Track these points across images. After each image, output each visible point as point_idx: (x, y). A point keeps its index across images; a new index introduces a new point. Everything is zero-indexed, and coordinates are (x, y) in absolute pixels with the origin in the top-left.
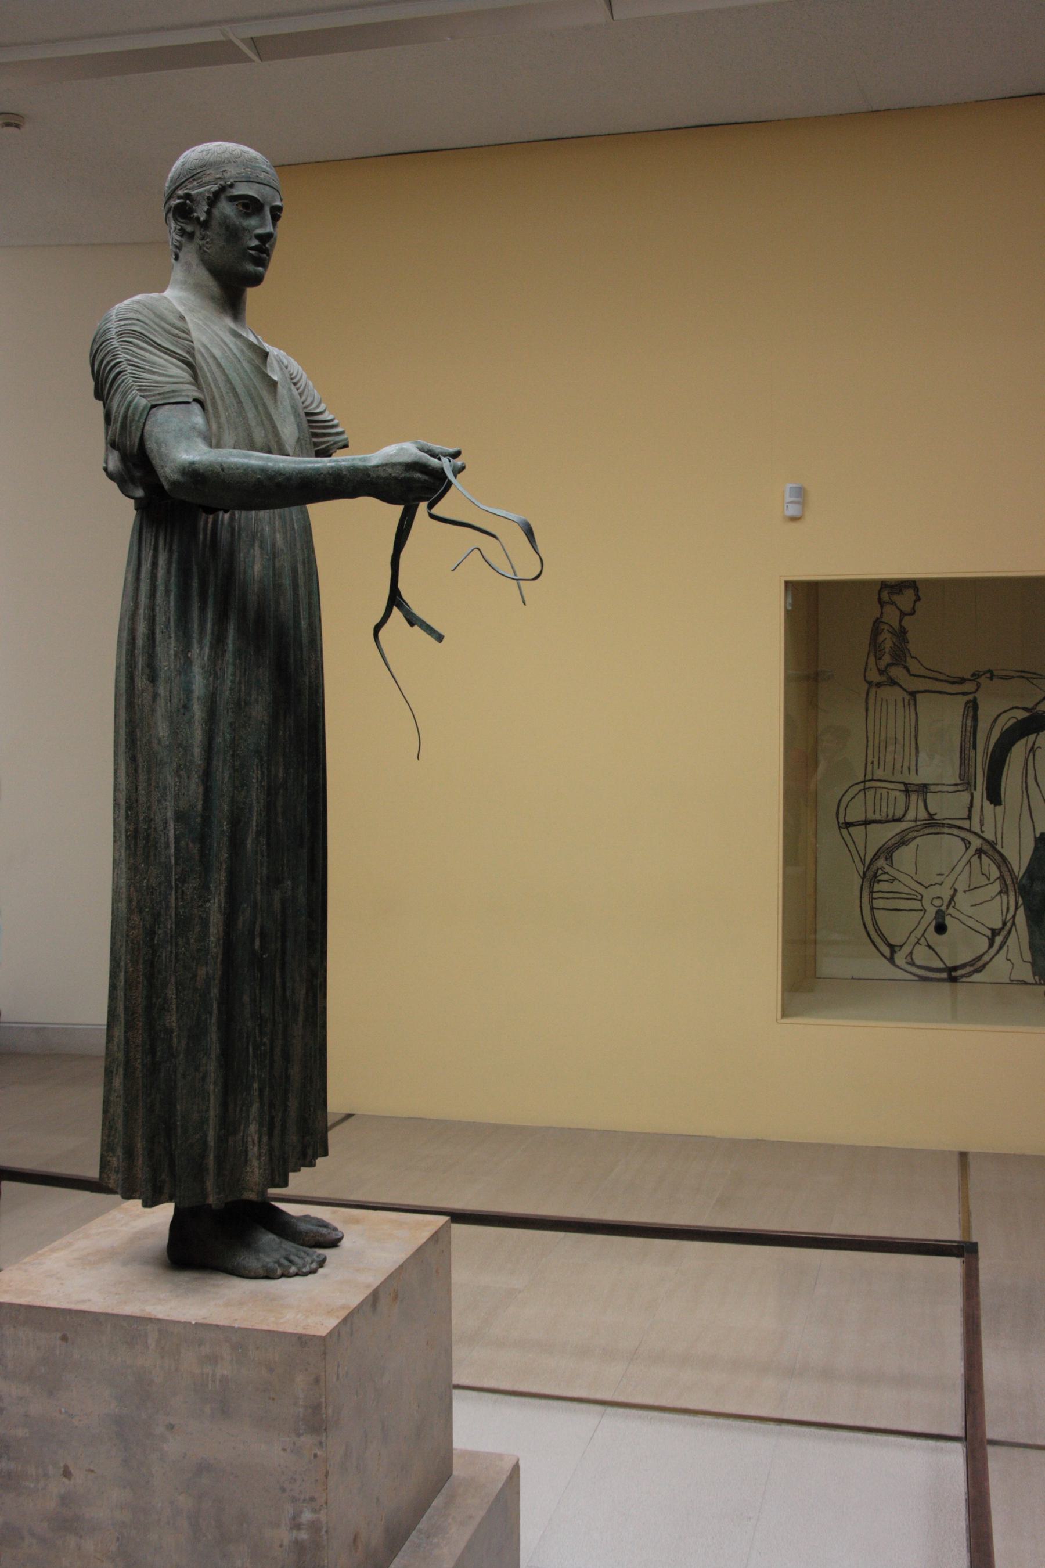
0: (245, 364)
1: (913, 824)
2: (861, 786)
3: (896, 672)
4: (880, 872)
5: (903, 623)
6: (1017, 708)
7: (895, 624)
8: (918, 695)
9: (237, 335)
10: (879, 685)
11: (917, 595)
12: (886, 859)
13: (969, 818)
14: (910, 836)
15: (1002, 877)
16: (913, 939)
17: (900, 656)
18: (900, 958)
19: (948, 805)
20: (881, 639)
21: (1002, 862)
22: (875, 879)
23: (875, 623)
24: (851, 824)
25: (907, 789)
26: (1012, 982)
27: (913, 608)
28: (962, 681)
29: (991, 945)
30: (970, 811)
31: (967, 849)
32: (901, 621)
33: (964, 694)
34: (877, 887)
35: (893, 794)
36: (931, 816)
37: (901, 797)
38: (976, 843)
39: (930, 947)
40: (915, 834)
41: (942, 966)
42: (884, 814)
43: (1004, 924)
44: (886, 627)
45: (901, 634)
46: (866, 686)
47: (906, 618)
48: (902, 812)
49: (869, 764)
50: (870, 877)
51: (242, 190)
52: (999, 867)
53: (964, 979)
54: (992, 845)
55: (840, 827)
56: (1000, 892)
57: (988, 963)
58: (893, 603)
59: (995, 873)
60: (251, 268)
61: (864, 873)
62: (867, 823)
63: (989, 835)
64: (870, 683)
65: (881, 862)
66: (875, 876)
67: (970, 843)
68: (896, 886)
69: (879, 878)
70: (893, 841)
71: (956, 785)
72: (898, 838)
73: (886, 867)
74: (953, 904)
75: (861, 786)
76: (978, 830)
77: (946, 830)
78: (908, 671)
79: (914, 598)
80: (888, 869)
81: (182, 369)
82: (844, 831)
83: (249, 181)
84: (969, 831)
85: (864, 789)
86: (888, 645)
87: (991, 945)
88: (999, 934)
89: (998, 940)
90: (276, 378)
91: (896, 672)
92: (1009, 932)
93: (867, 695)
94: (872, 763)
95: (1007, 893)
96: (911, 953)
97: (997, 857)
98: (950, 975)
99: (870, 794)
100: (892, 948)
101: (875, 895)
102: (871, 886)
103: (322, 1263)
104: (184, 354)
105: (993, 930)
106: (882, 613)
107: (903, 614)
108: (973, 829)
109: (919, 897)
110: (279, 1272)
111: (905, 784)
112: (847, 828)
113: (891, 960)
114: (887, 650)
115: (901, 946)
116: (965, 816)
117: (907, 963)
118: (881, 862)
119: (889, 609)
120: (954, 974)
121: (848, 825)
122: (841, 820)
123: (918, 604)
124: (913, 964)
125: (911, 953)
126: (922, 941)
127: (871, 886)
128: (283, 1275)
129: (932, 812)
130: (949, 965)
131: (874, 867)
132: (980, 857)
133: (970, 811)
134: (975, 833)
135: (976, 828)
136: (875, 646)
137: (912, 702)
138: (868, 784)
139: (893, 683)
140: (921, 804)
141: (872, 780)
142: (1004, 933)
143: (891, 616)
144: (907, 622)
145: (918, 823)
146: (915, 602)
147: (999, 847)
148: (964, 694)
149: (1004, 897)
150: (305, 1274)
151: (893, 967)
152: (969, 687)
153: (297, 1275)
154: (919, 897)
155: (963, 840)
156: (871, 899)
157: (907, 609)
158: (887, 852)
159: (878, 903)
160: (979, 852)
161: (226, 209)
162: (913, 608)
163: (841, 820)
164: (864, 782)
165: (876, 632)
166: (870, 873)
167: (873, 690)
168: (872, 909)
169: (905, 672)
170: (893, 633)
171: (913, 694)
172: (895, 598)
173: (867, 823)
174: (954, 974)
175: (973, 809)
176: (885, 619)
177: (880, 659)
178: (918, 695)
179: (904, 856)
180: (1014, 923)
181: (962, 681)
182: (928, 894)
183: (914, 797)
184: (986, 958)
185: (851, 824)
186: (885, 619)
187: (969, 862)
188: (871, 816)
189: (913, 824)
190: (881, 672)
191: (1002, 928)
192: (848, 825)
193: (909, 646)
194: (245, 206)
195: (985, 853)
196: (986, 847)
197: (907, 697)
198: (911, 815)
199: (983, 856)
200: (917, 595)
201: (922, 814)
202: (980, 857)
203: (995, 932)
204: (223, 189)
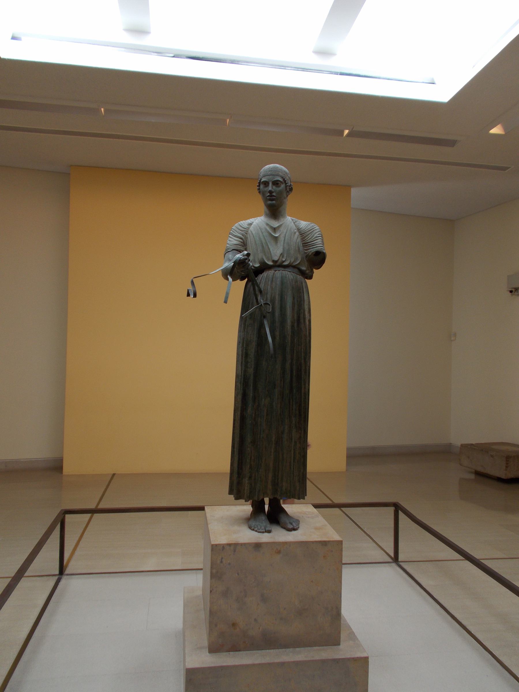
0: (265, 234)
9: (267, 224)
51: (263, 180)
60: (270, 202)
81: (237, 241)
83: (264, 176)
90: (277, 235)
103: (269, 532)
104: (241, 236)
110: (253, 528)
128: (253, 530)
150: (259, 532)
153: (256, 531)
161: (262, 186)
194: (265, 184)
204: (260, 181)
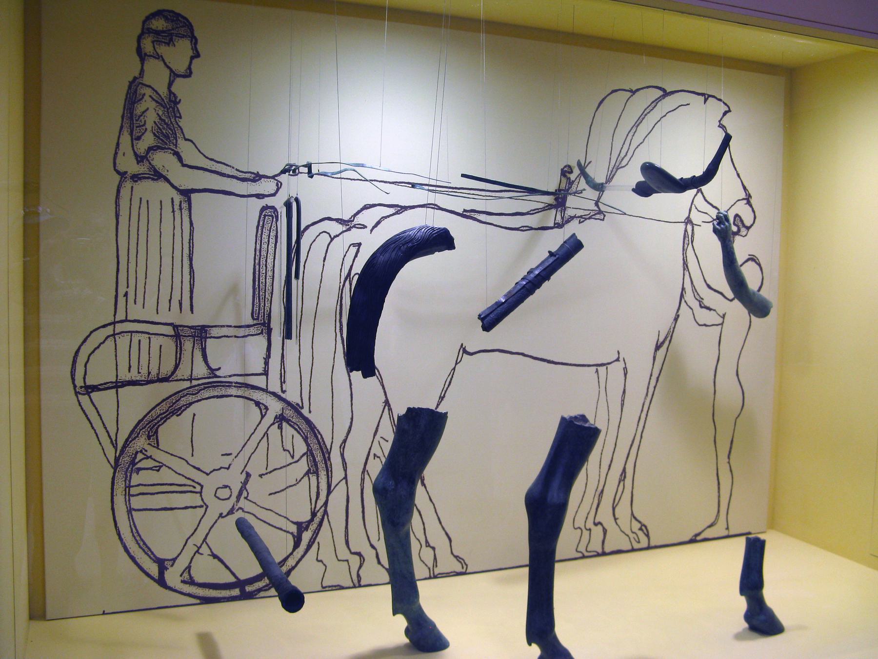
1: (187, 384)
2: (109, 330)
3: (163, 160)
4: (140, 456)
5: (173, 89)
6: (329, 219)
7: (163, 91)
8: (194, 196)
10: (136, 178)
11: (195, 48)
12: (149, 437)
13: (266, 373)
14: (183, 401)
15: (309, 453)
16: (190, 549)
17: (168, 136)
18: (173, 577)
19: (233, 356)
20: (139, 108)
21: (310, 431)
22: (133, 467)
23: (131, 83)
24: (95, 388)
25: (178, 333)
26: (324, 589)
27: (189, 68)
28: (257, 177)
29: (297, 545)
30: (267, 363)
31: (263, 417)
32: (170, 84)
33: (259, 196)
34: (136, 479)
35: (156, 341)
36: (213, 372)
37: (170, 346)
38: (275, 407)
39: (215, 556)
40: (191, 398)
41: (232, 579)
42: (144, 371)
43: (314, 514)
44: (148, 92)
45: (171, 104)
46: (117, 178)
47: (179, 81)
48: (171, 367)
49: (121, 300)
50: (125, 463)
52: (306, 439)
53: (262, 594)
54: (297, 409)
55: (77, 393)
56: (307, 473)
57: (293, 568)
58: (159, 57)
59: (301, 447)
61: (117, 460)
62: (118, 385)
63: (293, 396)
64: (122, 175)
65: (141, 442)
66: (133, 463)
67: (267, 408)
68: (166, 476)
69: (138, 466)
70: (158, 411)
71: (248, 326)
72: (165, 406)
73: (147, 447)
74: (245, 494)
75: (109, 330)
76: (278, 390)
77: (233, 391)
78: (180, 159)
79: (190, 53)
80: (151, 451)
82: (84, 399)
84: (266, 391)
85: (114, 335)
86: (151, 119)
87: (297, 545)
88: (307, 529)
89: (306, 536)
91: (163, 160)
92: (320, 524)
93: (118, 191)
94: (126, 295)
95: (316, 473)
96: (189, 568)
97: (304, 426)
98: (243, 590)
99: (123, 342)
100: (162, 565)
101: (133, 491)
102: (127, 478)
105: (299, 524)
106: (142, 71)
107: (174, 75)
108: (270, 389)
109: (198, 489)
111: (175, 327)
112: (88, 394)
113: (161, 581)
114: (149, 125)
115: (174, 560)
116: (261, 371)
117: (183, 582)
118: (141, 442)
119: (151, 65)
120: (248, 589)
121: (90, 389)
122: (79, 382)
123: (195, 61)
124: (191, 582)
125: (189, 568)
126: (204, 549)
127: (127, 478)
129: (214, 367)
130: (242, 577)
131: (130, 450)
132: (280, 427)
133: (267, 363)
134: (274, 394)
135: (275, 387)
136: (131, 118)
137: (185, 205)
138: (119, 328)
139: (157, 175)
140: (198, 354)
141: (126, 320)
142: (313, 527)
143: (156, 77)
144: (179, 86)
145: (195, 383)
146: (192, 58)
147: (305, 412)
148: (259, 196)
149: (313, 478)
151: (164, 590)
152: (267, 187)
154: (198, 489)
155: (258, 404)
156: (128, 495)
157: (181, 68)
158: (150, 427)
159: (136, 502)
160: (281, 419)
162: (189, 68)
163: (79, 382)
164: (114, 323)
165: (132, 98)
166: (125, 460)
167: (128, 184)
168: (130, 511)
169: (174, 159)
170: (160, 103)
171: (187, 194)
172: (162, 50)
173: (118, 385)
174: (248, 589)
175: (271, 361)
176: (146, 80)
177: (139, 138)
178: (194, 196)
179: (173, 432)
180: (326, 512)
181: (257, 177)
182: (209, 484)
183: (188, 345)
184: (291, 562)
185: (95, 388)
186: (146, 80)
187: (266, 433)
188: (124, 376)
189: (187, 384)
190: (140, 159)
191: (312, 520)
192: (90, 389)
193: (182, 123)
195: (288, 421)
196: (289, 413)
197: (178, 198)
198: (184, 371)
199: (284, 424)
200: (195, 48)
201: (200, 370)
202: (280, 427)
203: (302, 527)
